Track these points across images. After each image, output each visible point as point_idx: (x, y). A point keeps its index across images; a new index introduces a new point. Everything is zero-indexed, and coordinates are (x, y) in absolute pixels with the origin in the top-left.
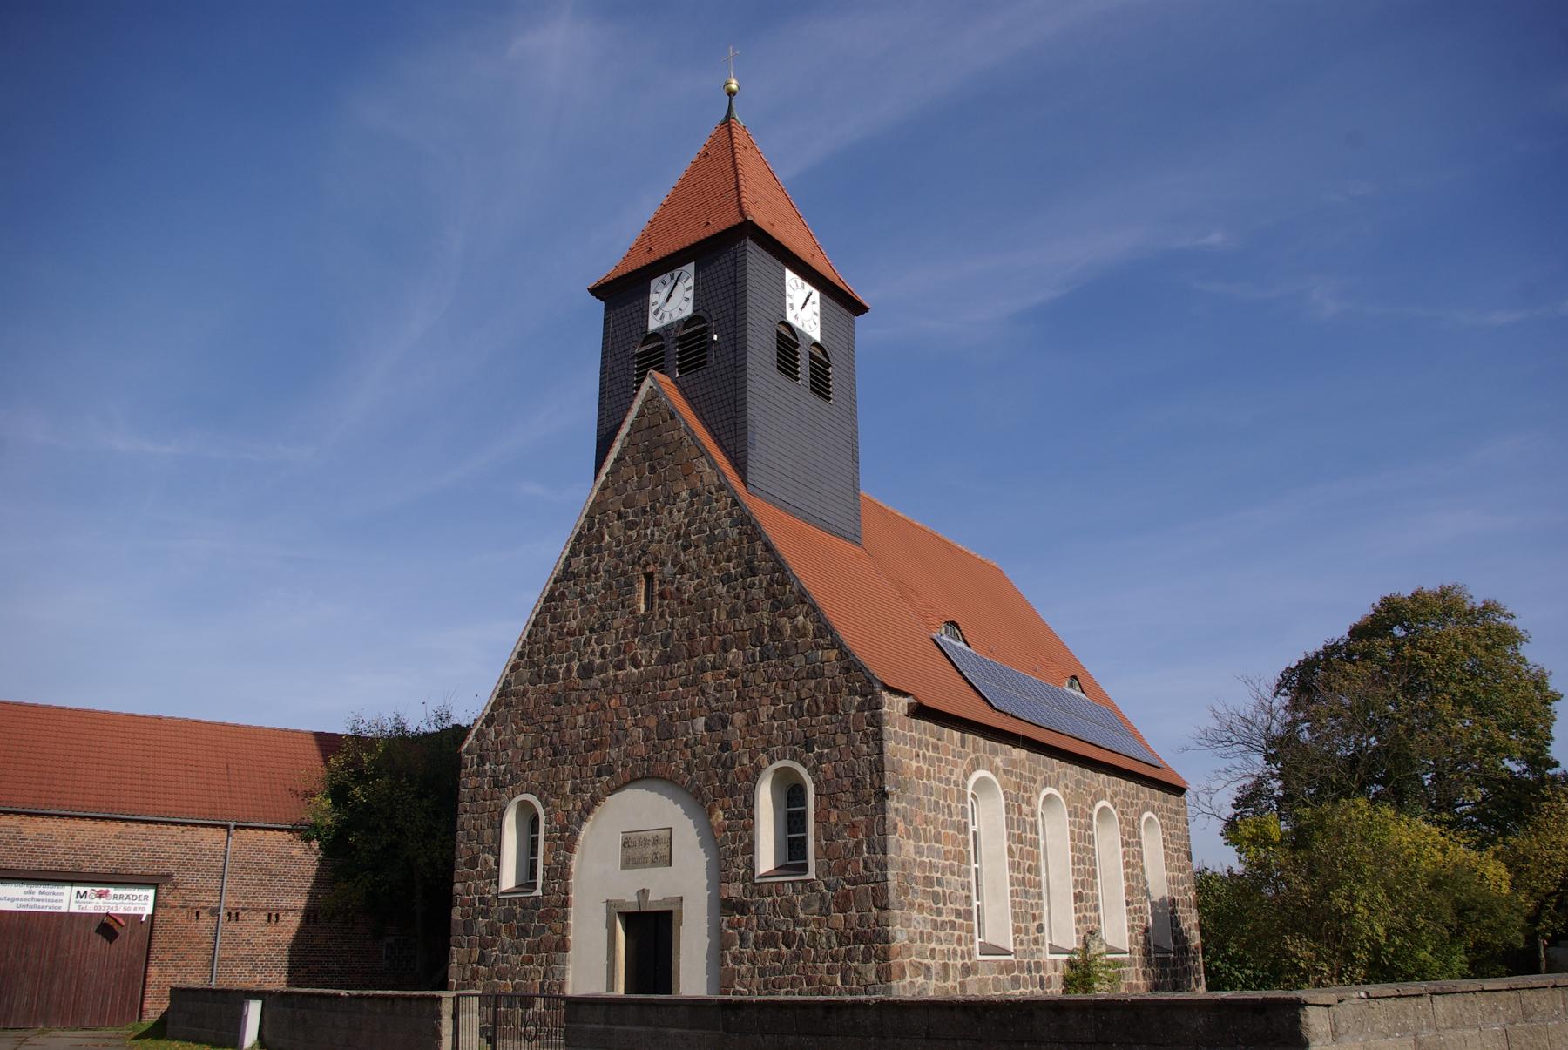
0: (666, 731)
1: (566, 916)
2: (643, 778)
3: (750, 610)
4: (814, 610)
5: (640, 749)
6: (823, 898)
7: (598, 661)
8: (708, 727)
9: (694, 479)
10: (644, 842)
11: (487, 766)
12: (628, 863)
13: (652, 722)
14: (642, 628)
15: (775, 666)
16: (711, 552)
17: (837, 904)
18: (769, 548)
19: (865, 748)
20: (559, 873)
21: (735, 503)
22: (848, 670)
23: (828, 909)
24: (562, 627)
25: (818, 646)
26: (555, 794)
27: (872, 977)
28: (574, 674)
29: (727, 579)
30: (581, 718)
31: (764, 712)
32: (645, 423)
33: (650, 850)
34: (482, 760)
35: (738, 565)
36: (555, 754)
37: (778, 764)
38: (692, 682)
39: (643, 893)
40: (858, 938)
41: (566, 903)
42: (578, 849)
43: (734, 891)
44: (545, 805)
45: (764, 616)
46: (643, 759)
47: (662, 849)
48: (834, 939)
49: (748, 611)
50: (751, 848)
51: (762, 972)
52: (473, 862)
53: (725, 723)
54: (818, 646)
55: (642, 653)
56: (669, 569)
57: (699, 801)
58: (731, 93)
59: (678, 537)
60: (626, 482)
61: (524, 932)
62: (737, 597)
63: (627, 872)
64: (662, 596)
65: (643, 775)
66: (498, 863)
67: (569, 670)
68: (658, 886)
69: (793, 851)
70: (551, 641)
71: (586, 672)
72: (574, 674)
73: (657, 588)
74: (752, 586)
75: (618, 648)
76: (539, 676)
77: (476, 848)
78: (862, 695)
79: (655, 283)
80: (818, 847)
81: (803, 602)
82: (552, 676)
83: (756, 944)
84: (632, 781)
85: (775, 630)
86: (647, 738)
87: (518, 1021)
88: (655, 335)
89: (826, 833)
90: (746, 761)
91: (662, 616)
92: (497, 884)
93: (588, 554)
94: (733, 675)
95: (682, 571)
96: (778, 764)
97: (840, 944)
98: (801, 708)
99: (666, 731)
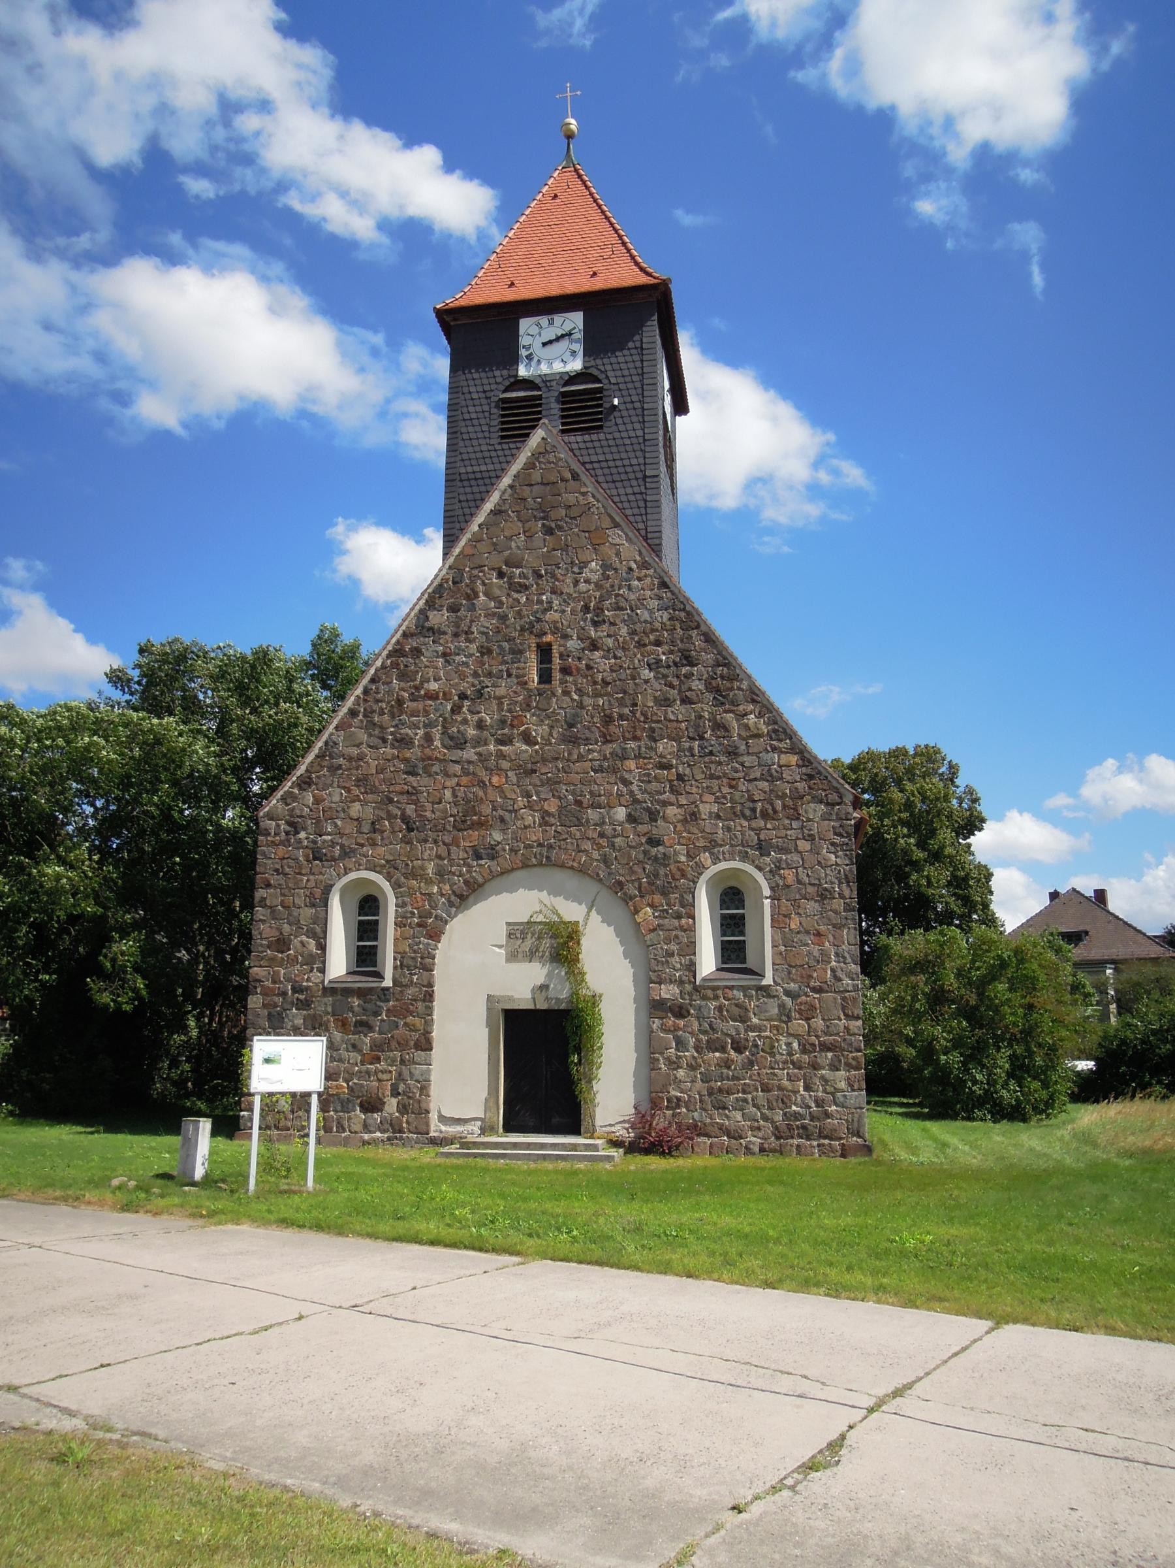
0: (572, 815)
1: (429, 1011)
2: (541, 865)
3: (685, 701)
4: (767, 709)
5: (535, 835)
6: (782, 1006)
7: (471, 732)
8: (631, 819)
9: (606, 549)
11: (302, 835)
13: (552, 806)
14: (536, 701)
15: (720, 763)
16: (633, 632)
17: (800, 1012)
18: (710, 639)
19: (833, 857)
20: (418, 964)
21: (664, 585)
22: (811, 777)
23: (789, 1017)
24: (417, 688)
25: (774, 749)
26: (413, 874)
27: (843, 1085)
28: (437, 743)
29: (655, 665)
30: (448, 794)
31: (707, 808)
32: (536, 476)
34: (295, 827)
35: (671, 652)
36: (410, 830)
37: (723, 865)
38: (612, 767)
40: (826, 1048)
41: (429, 997)
42: (444, 938)
43: (668, 992)
44: (396, 886)
45: (706, 709)
46: (540, 845)
48: (795, 1045)
49: (683, 701)
50: (690, 948)
51: (706, 1079)
52: (282, 944)
53: (653, 816)
54: (774, 749)
55: (539, 731)
56: (573, 644)
58: (570, 136)
59: (586, 609)
60: (510, 538)
61: (364, 1026)
62: (671, 686)
63: (515, 966)
64: (565, 671)
65: (539, 860)
66: (323, 947)
67: (428, 738)
69: (733, 953)
70: (400, 702)
71: (459, 743)
72: (437, 743)
73: (556, 661)
74: (689, 676)
75: (503, 722)
76: (384, 740)
77: (286, 928)
78: (827, 804)
79: (526, 325)
80: (776, 954)
81: (753, 701)
82: (403, 742)
83: (697, 1048)
85: (720, 727)
86: (544, 823)
87: (357, 1127)
88: (528, 384)
89: (786, 941)
90: (683, 859)
91: (566, 693)
92: (322, 971)
93: (454, 609)
94: (668, 767)
95: (594, 646)
96: (723, 865)
97: (804, 1051)
98: (753, 810)
99: (572, 815)
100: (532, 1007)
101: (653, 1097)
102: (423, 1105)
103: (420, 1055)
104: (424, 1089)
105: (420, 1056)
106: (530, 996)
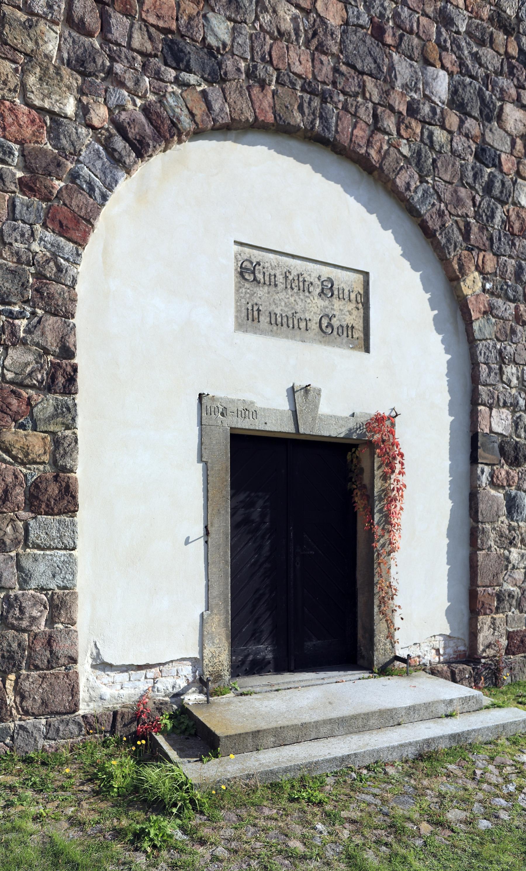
1: (67, 414)
10: (300, 284)
12: (250, 317)
33: (314, 306)
39: (301, 395)
47: (346, 314)
57: (434, 244)
68: (342, 392)
84: (276, 130)
100: (288, 428)
101: (473, 598)
102: (62, 648)
103: (44, 526)
104: (59, 606)
105: (45, 527)
106: (284, 405)
